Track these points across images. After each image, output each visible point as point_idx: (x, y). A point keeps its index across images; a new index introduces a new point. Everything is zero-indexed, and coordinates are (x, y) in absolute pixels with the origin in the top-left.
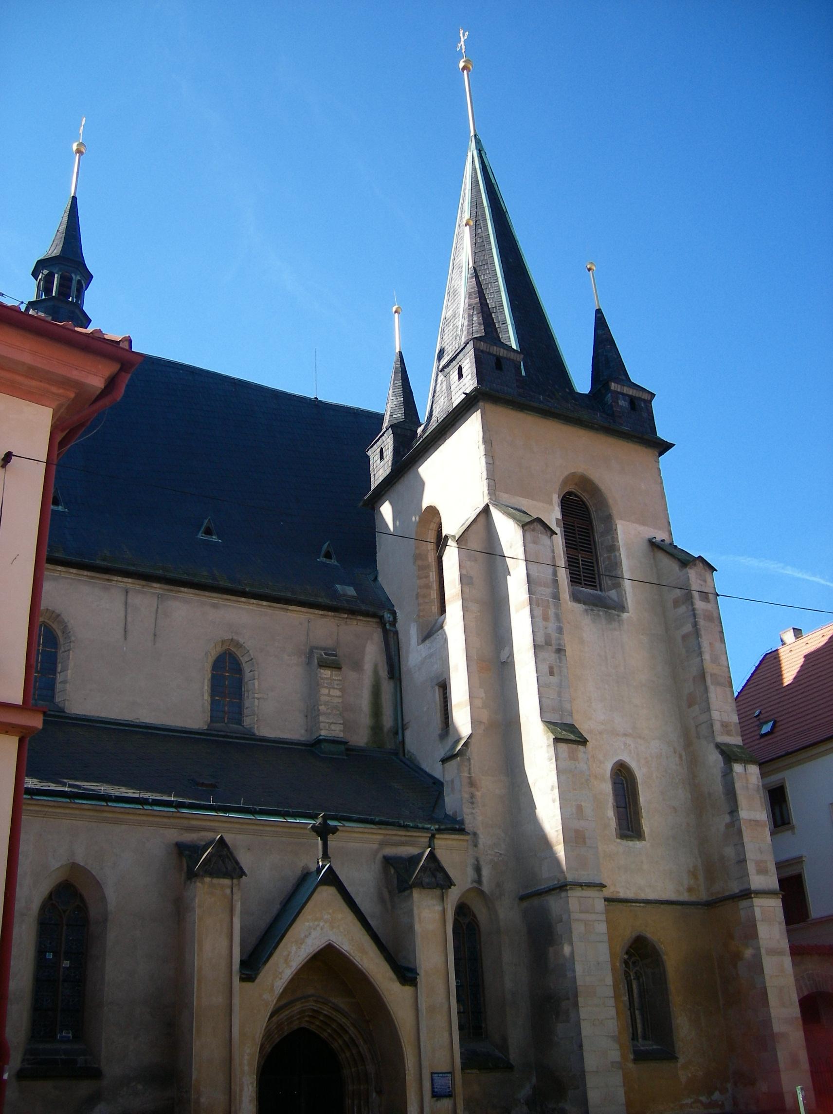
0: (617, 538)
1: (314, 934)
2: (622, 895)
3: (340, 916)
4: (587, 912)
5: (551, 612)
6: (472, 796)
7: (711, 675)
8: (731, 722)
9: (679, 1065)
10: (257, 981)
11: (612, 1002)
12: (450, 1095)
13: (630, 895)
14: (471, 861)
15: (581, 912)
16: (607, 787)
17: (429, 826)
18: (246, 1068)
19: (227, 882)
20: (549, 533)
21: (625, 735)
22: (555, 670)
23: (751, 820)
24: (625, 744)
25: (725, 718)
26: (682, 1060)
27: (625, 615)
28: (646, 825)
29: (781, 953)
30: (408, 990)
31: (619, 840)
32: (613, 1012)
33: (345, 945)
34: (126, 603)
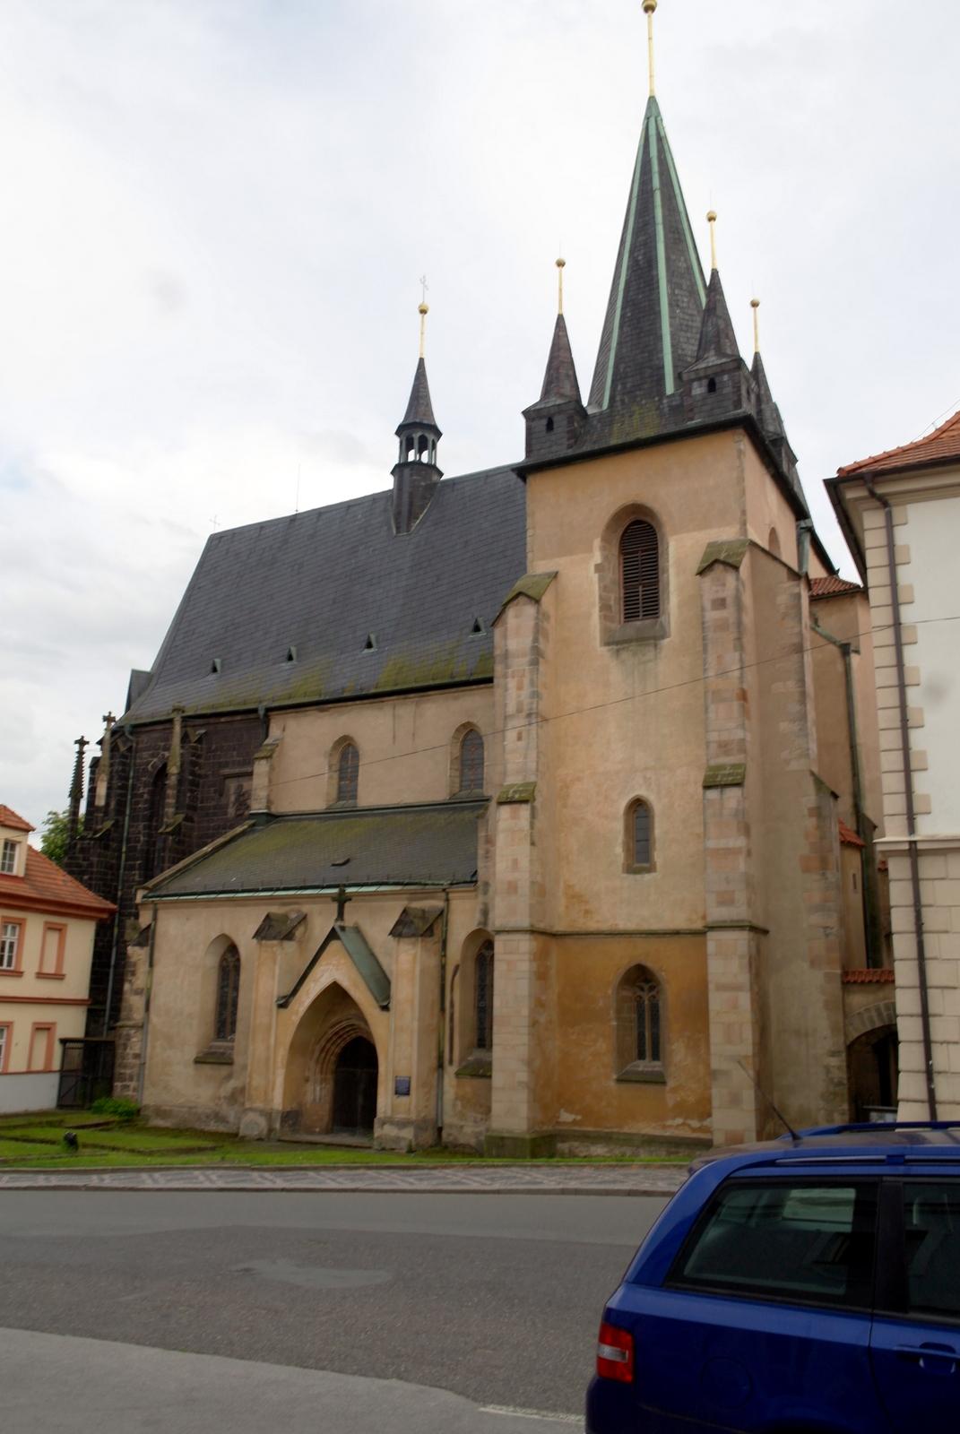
0: (668, 558)
1: (326, 975)
2: (623, 925)
3: (343, 961)
4: (511, 953)
5: (526, 681)
6: (487, 852)
7: (713, 693)
8: (733, 740)
9: (668, 1088)
10: (289, 1008)
11: (525, 1030)
12: (407, 1093)
13: (631, 926)
14: (480, 907)
15: (505, 953)
16: (619, 826)
17: (441, 882)
18: (279, 1064)
19: (275, 942)
20: (533, 602)
21: (646, 769)
22: (524, 735)
23: (718, 850)
24: (645, 777)
25: (725, 737)
26: (671, 1083)
27: (666, 641)
28: (658, 857)
29: (736, 988)
30: (385, 1013)
31: (625, 875)
32: (525, 1039)
33: (345, 983)
34: (394, 716)
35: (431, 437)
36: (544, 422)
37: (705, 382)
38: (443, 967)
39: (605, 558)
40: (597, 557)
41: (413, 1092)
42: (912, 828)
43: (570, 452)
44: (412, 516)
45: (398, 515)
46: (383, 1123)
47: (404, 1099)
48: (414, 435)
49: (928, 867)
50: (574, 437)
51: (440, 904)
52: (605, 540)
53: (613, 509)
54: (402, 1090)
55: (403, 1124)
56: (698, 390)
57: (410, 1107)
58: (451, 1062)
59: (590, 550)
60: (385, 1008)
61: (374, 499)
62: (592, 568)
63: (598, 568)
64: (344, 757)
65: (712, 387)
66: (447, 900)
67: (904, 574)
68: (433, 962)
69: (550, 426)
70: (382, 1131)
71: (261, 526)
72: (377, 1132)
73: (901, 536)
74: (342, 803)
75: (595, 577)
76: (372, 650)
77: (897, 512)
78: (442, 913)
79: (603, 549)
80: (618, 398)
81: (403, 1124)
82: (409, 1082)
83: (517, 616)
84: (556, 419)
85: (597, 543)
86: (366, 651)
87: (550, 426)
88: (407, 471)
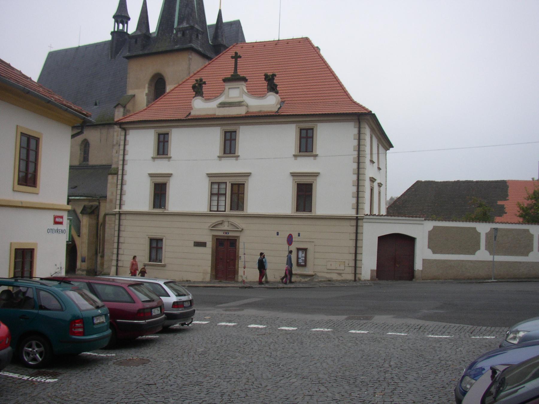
12: (85, 261)
35: (125, 20)
36: (134, 40)
37: (182, 32)
38: (97, 223)
39: (149, 91)
40: (146, 91)
41: (86, 261)
42: (120, 208)
44: (117, 53)
46: (78, 270)
47: (84, 263)
48: (119, 20)
49: (123, 217)
50: (144, 47)
51: (97, 203)
52: (150, 85)
53: (152, 74)
54: (83, 260)
55: (83, 270)
56: (180, 35)
57: (85, 265)
58: (100, 253)
59: (145, 88)
60: (79, 236)
61: (105, 43)
62: (145, 94)
63: (147, 95)
64: (85, 147)
65: (183, 35)
66: (99, 203)
67: (127, 147)
68: (94, 222)
69: (136, 42)
70: (78, 272)
71: (66, 51)
72: (77, 273)
73: (128, 138)
74: (84, 163)
75: (145, 97)
76: (97, 107)
77: (127, 131)
78: (97, 207)
79: (149, 88)
80: (160, 32)
81: (83, 270)
82: (85, 258)
83: (118, 111)
85: (147, 85)
86: (95, 107)
87: (136, 42)
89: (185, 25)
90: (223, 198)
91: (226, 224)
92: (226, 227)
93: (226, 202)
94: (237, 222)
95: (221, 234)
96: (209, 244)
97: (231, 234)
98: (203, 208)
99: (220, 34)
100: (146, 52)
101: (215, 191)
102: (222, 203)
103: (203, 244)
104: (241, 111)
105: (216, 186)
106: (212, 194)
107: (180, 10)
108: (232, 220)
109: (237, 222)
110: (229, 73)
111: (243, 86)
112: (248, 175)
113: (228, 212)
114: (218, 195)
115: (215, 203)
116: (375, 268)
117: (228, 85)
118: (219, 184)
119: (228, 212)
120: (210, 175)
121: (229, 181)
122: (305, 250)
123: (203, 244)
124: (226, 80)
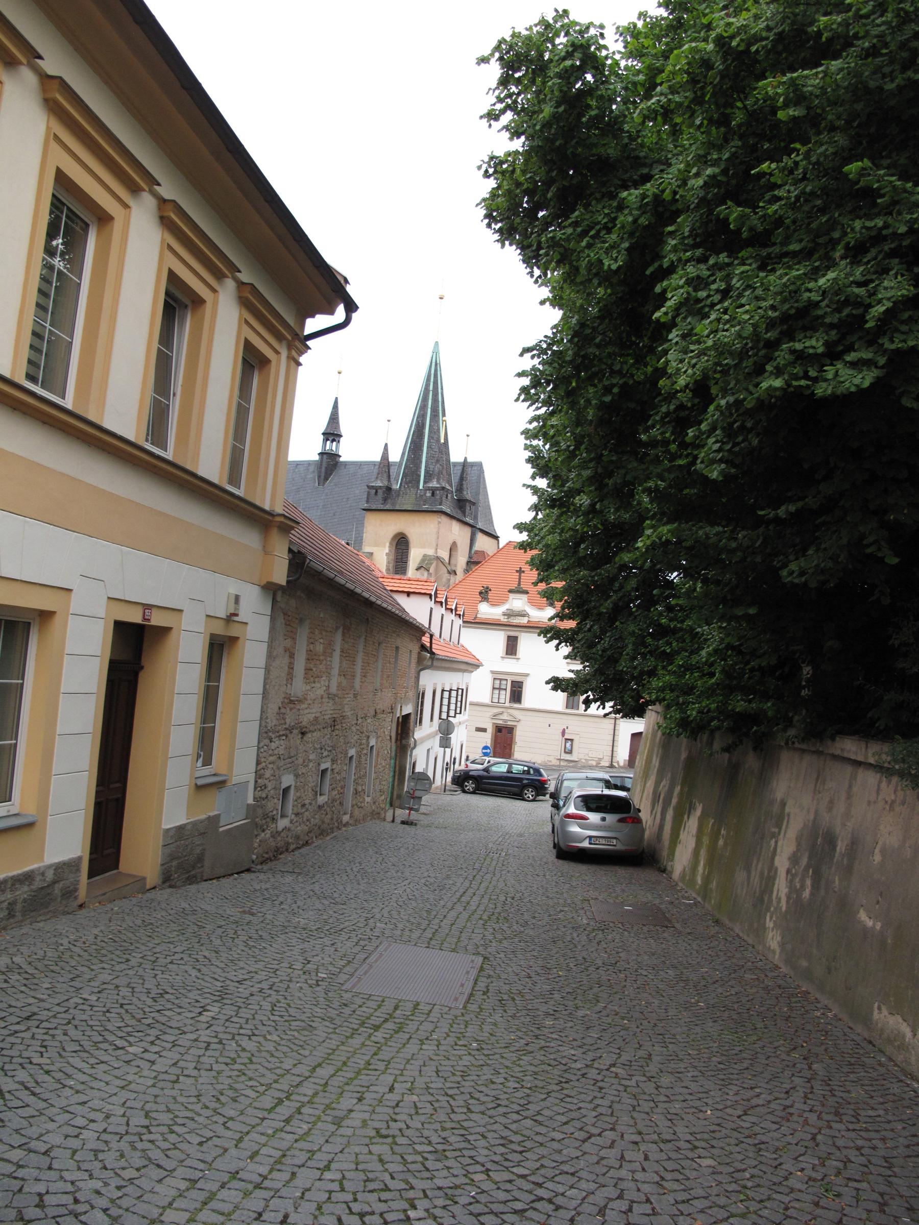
40: (387, 550)
43: (381, 507)
44: (326, 479)
45: (319, 477)
50: (385, 500)
52: (391, 544)
56: (429, 494)
61: (309, 463)
65: (433, 494)
69: (376, 493)
75: (385, 557)
84: (379, 491)
85: (388, 544)
88: (325, 456)
89: (434, 484)
90: (503, 692)
91: (505, 714)
92: (505, 717)
93: (506, 696)
94: (518, 714)
95: (501, 722)
96: (490, 730)
97: (509, 723)
98: (487, 700)
99: (465, 486)
100: (387, 507)
101: (497, 686)
102: (503, 697)
103: (484, 730)
104: (524, 621)
105: (497, 682)
106: (494, 688)
107: (426, 461)
108: (510, 711)
109: (518, 714)
110: (514, 586)
111: (525, 597)
112: (527, 675)
113: (507, 704)
114: (500, 689)
115: (496, 696)
116: (627, 758)
117: (512, 596)
118: (501, 680)
119: (507, 704)
120: (493, 672)
121: (510, 679)
122: (572, 740)
123: (484, 730)
124: (511, 591)
